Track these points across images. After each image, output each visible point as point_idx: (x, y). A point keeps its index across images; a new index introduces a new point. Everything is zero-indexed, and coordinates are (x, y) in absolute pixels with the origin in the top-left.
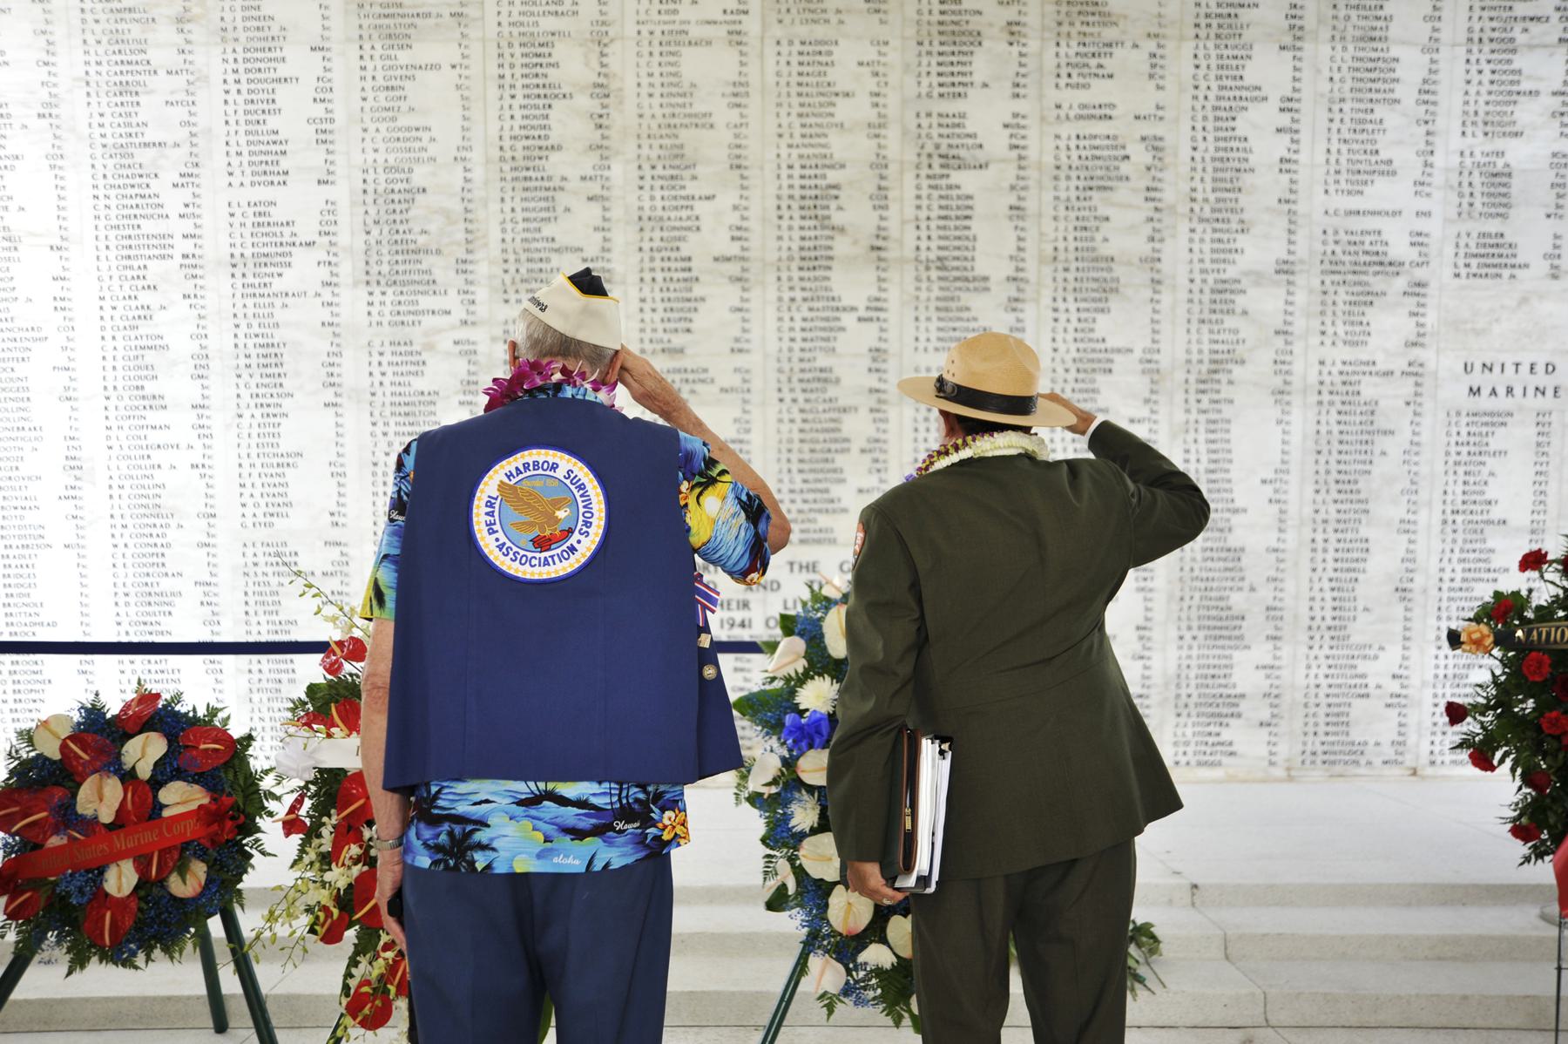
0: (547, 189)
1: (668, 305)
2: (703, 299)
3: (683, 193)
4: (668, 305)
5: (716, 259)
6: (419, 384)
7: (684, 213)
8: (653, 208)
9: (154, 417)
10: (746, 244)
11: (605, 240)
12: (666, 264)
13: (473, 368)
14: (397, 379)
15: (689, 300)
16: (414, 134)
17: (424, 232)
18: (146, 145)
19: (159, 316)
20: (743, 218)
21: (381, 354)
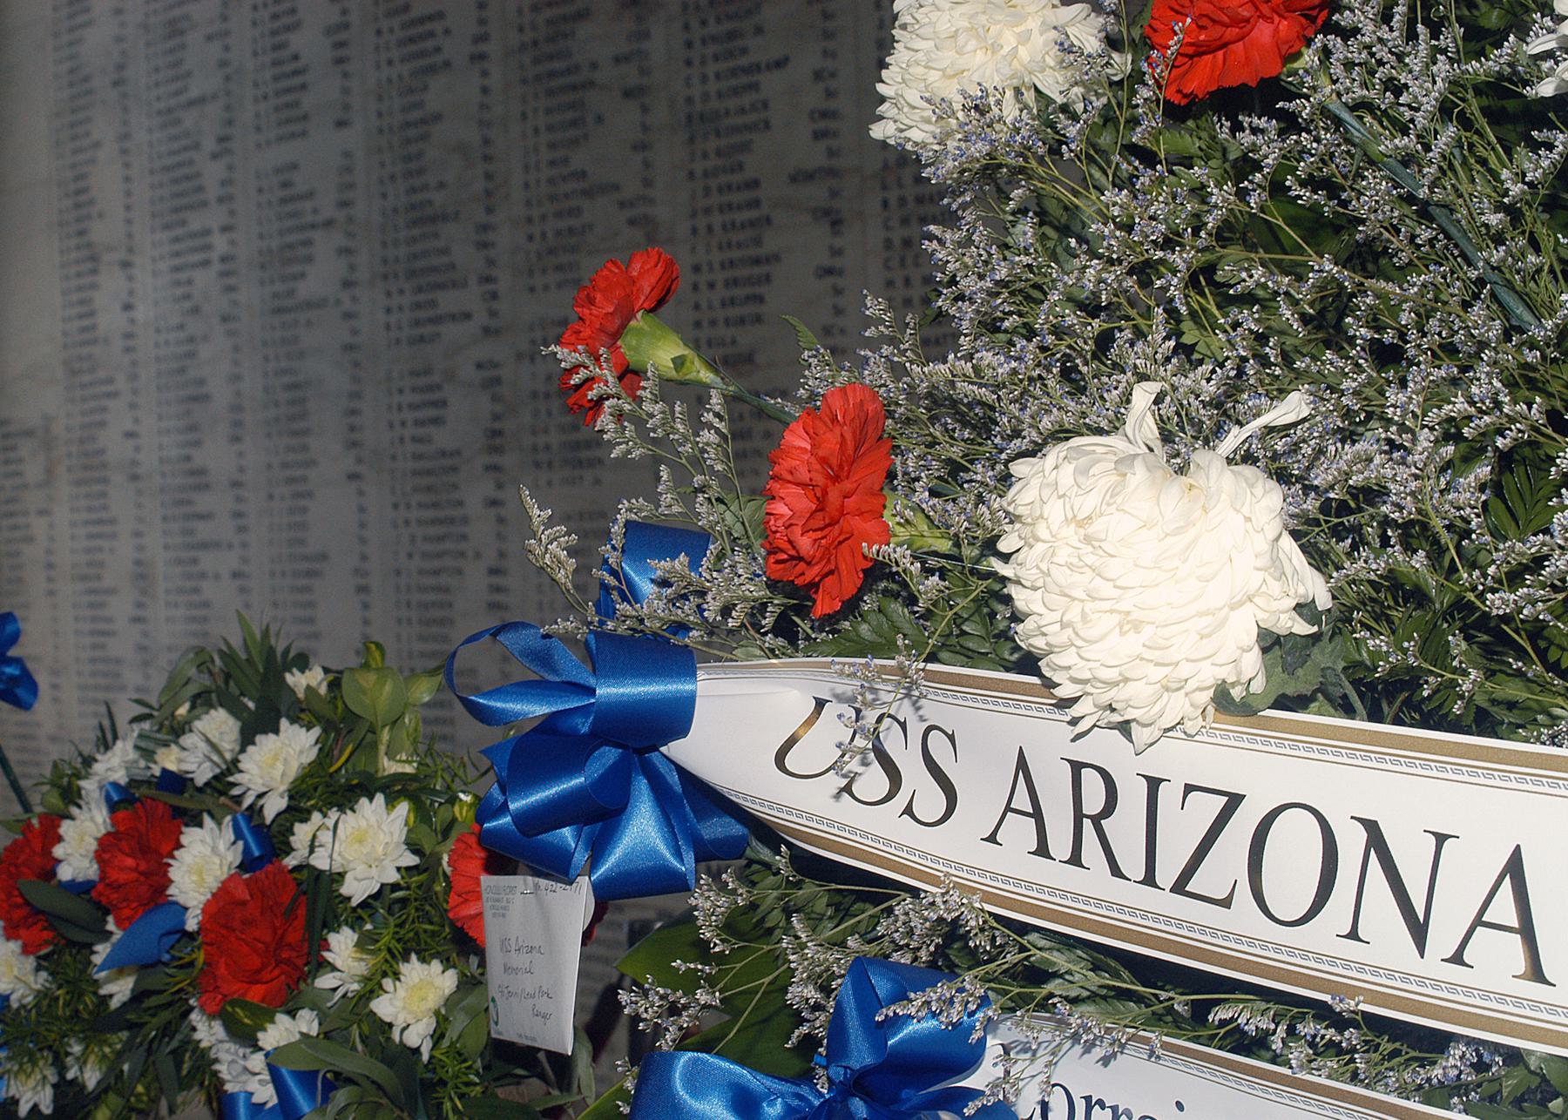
0: (574, 88)
1: (730, 274)
2: (775, 258)
3: (744, 61)
4: (730, 274)
5: (794, 179)
6: (443, 438)
7: (747, 99)
8: (706, 96)
9: (203, 502)
10: (834, 143)
11: (647, 164)
12: (726, 198)
13: (498, 408)
14: (420, 431)
15: (757, 261)
16: (428, 26)
17: (442, 185)
18: (191, 103)
19: (205, 351)
20: (830, 94)
21: (401, 391)
